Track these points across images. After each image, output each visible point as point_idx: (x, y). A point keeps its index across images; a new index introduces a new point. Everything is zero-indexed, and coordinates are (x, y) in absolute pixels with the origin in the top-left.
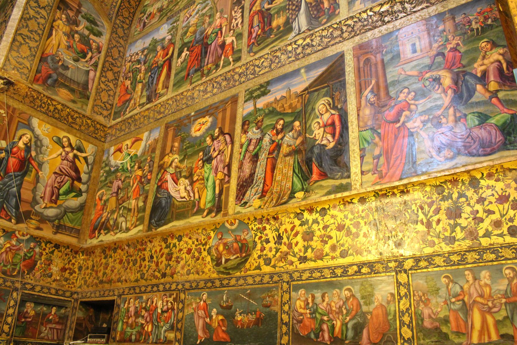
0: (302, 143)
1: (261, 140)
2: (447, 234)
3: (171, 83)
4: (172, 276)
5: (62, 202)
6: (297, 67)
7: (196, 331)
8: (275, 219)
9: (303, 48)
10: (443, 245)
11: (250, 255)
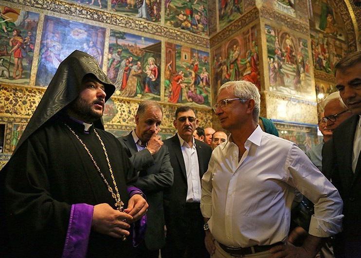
0: (141, 73)
1: (120, 62)
8: (128, 103)
9: (144, 26)
11: (115, 116)
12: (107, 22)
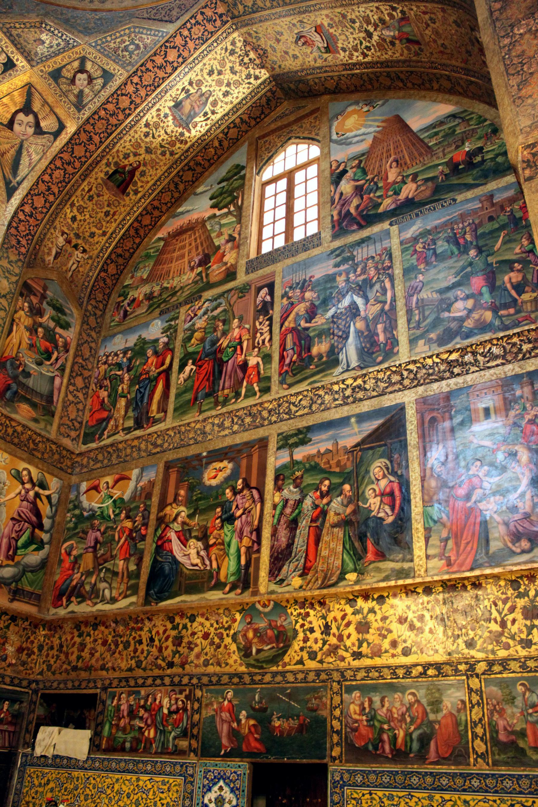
0: (354, 512)
1: (299, 503)
2: (524, 636)
3: (171, 407)
4: (182, 666)
5: (21, 557)
6: (345, 414)
7: (219, 738)
8: (322, 604)
9: (353, 389)
10: (519, 648)
12: (271, 423)
